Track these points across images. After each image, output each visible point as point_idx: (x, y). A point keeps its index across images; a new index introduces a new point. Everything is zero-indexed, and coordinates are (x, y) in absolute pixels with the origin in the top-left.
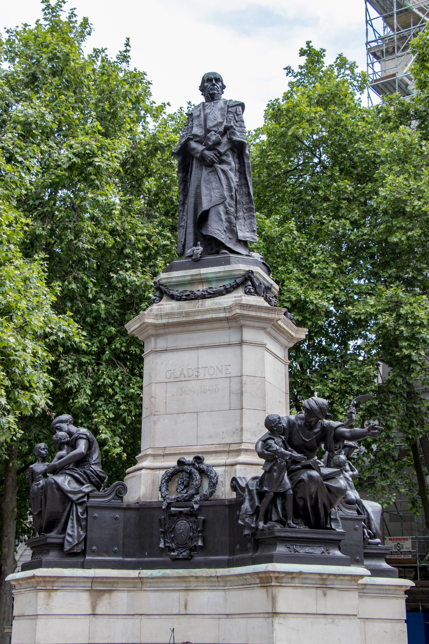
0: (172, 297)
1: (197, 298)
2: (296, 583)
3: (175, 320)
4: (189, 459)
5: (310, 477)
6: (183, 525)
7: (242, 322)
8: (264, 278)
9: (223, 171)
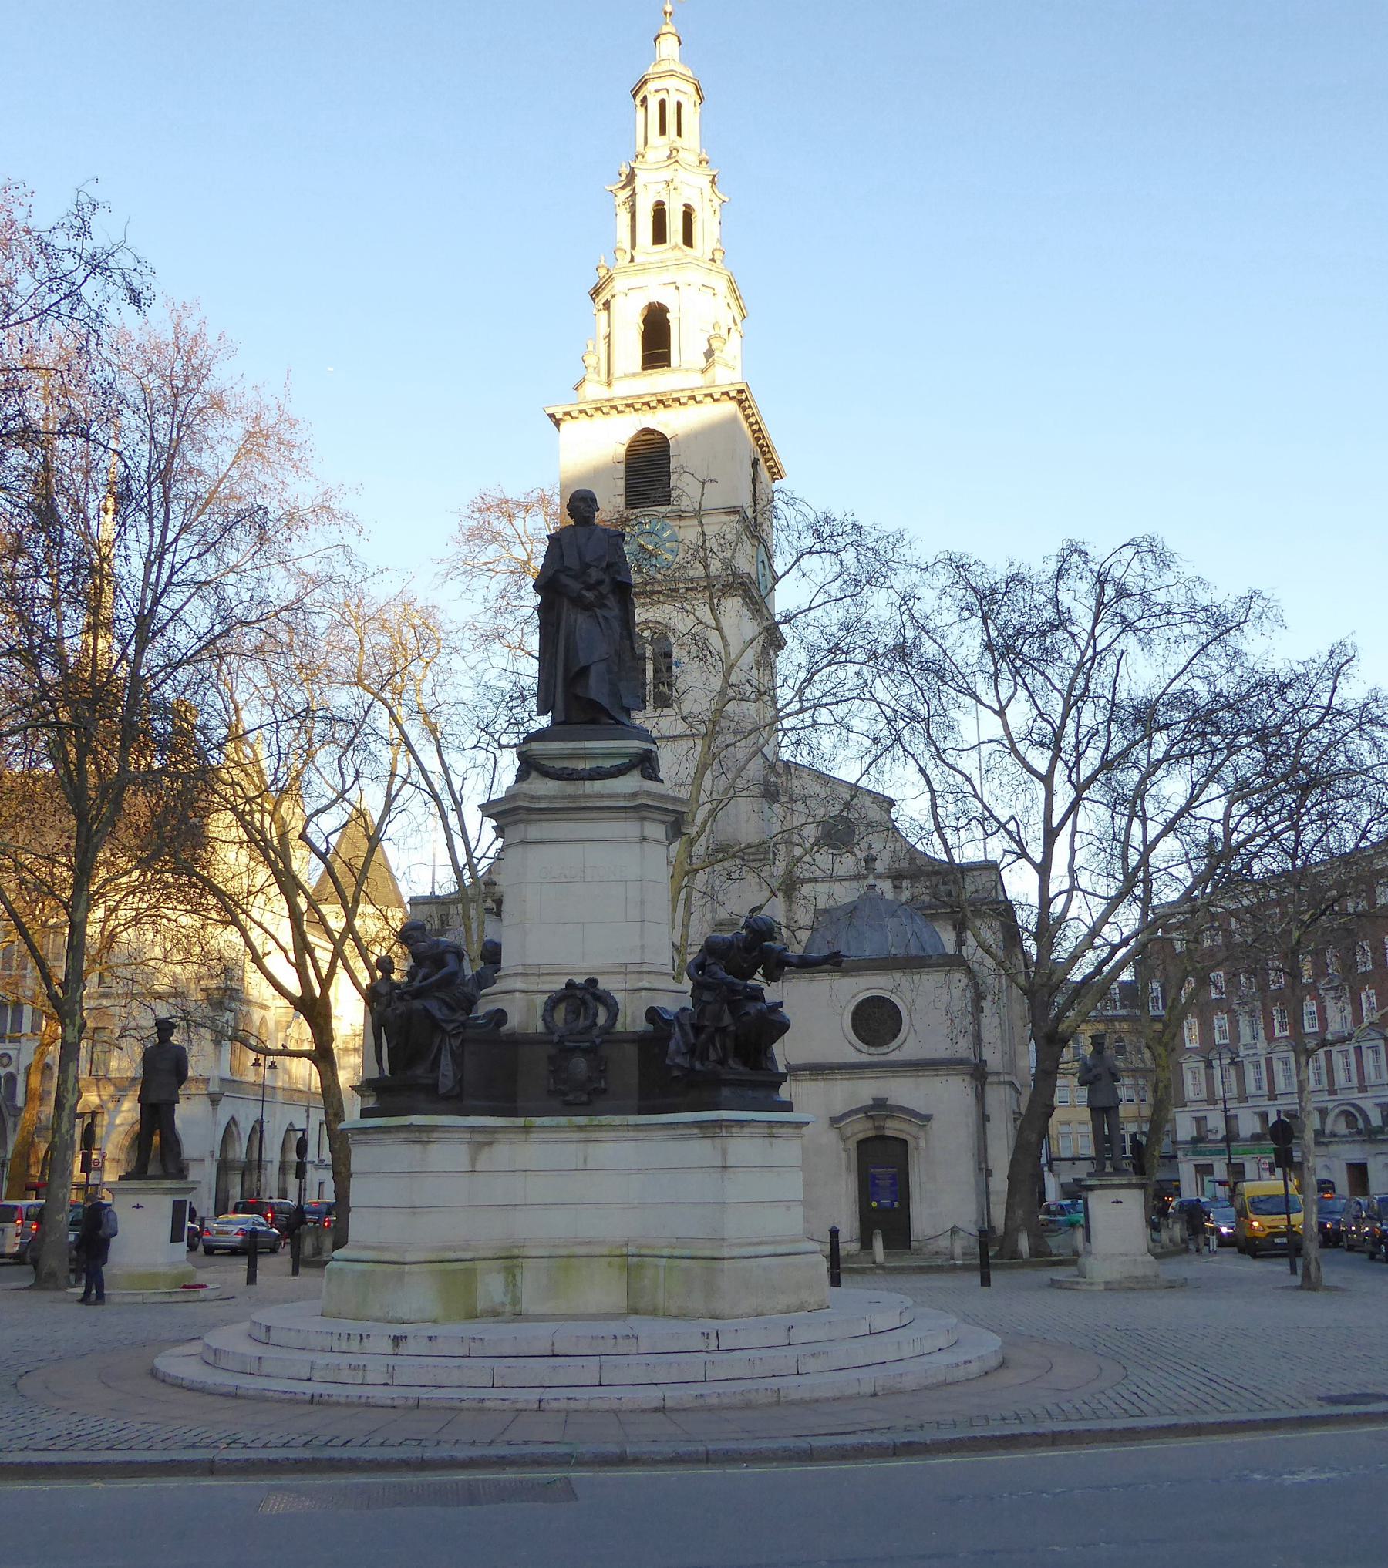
2: (746, 1131)
4: (579, 980)
7: (645, 814)
9: (605, 618)
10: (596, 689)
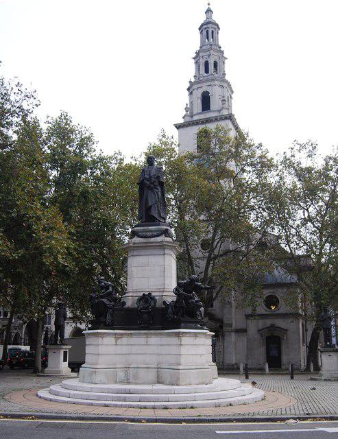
0: (139, 236)
1: (149, 237)
5: (193, 302)
6: (145, 316)
10: (154, 213)
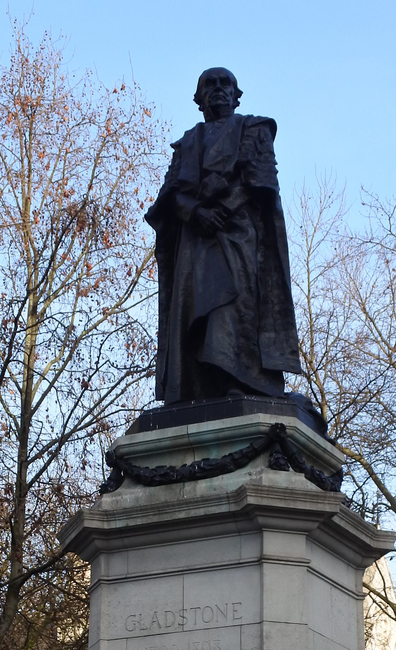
3: (139, 522)
7: (261, 520)
8: (308, 438)
9: (234, 245)
